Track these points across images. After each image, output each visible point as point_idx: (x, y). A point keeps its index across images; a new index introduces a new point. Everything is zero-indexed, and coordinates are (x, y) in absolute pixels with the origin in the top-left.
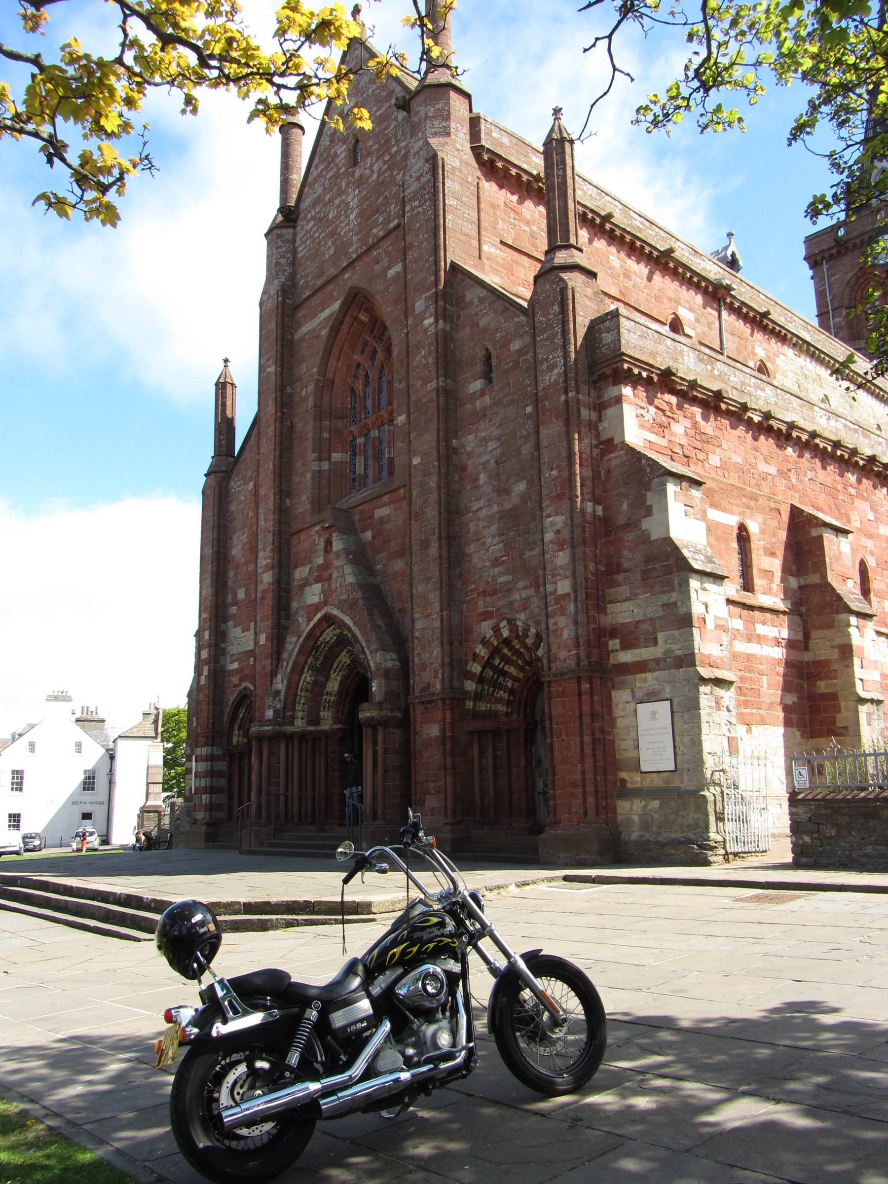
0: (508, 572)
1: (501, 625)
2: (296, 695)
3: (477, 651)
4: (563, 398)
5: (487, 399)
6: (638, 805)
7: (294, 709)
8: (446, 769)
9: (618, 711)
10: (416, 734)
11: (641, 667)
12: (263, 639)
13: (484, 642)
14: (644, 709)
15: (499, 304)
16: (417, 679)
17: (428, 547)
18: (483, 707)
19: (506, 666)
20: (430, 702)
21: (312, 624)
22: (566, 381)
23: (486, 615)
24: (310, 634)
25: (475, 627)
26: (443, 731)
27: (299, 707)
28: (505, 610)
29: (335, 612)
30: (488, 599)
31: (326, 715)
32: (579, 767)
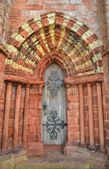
1: (49, 16)
3: (23, 27)
13: (31, 22)
18: (16, 66)
19: (38, 46)
25: (23, 12)
28: (56, 7)
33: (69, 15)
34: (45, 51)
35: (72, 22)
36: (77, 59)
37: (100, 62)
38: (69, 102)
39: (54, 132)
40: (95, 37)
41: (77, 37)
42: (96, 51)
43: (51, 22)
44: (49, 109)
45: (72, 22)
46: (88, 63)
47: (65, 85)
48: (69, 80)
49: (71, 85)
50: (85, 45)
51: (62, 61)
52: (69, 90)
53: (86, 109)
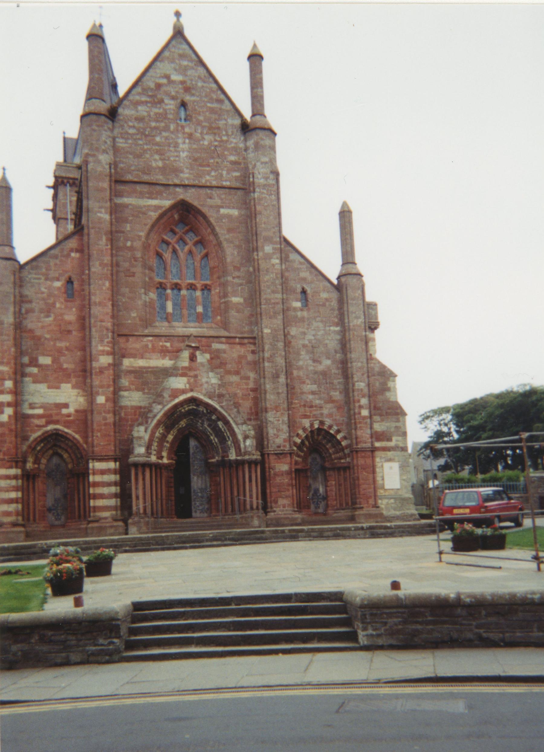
0: (320, 399)
2: (153, 440)
4: (364, 333)
5: (305, 314)
6: (385, 501)
7: (151, 449)
8: (292, 486)
9: (378, 465)
10: (269, 468)
11: (385, 449)
12: (101, 399)
13: (304, 429)
14: (387, 465)
15: (313, 270)
16: (271, 442)
17: (278, 377)
20: (281, 454)
21: (177, 401)
22: (365, 326)
23: (306, 416)
24: (176, 406)
26: (291, 468)
27: (153, 448)
29: (201, 397)
30: (307, 409)
31: (164, 454)
32: (373, 486)
33: (328, 422)
34: (309, 443)
35: (330, 427)
36: (333, 449)
37: (349, 454)
38: (328, 481)
39: (317, 504)
40: (345, 438)
41: (333, 437)
42: (347, 447)
43: (316, 426)
44: (313, 487)
45: (330, 427)
46: (341, 454)
47: (324, 469)
48: (327, 465)
49: (329, 469)
50: (339, 442)
51: (321, 450)
52: (328, 472)
53: (340, 485)
